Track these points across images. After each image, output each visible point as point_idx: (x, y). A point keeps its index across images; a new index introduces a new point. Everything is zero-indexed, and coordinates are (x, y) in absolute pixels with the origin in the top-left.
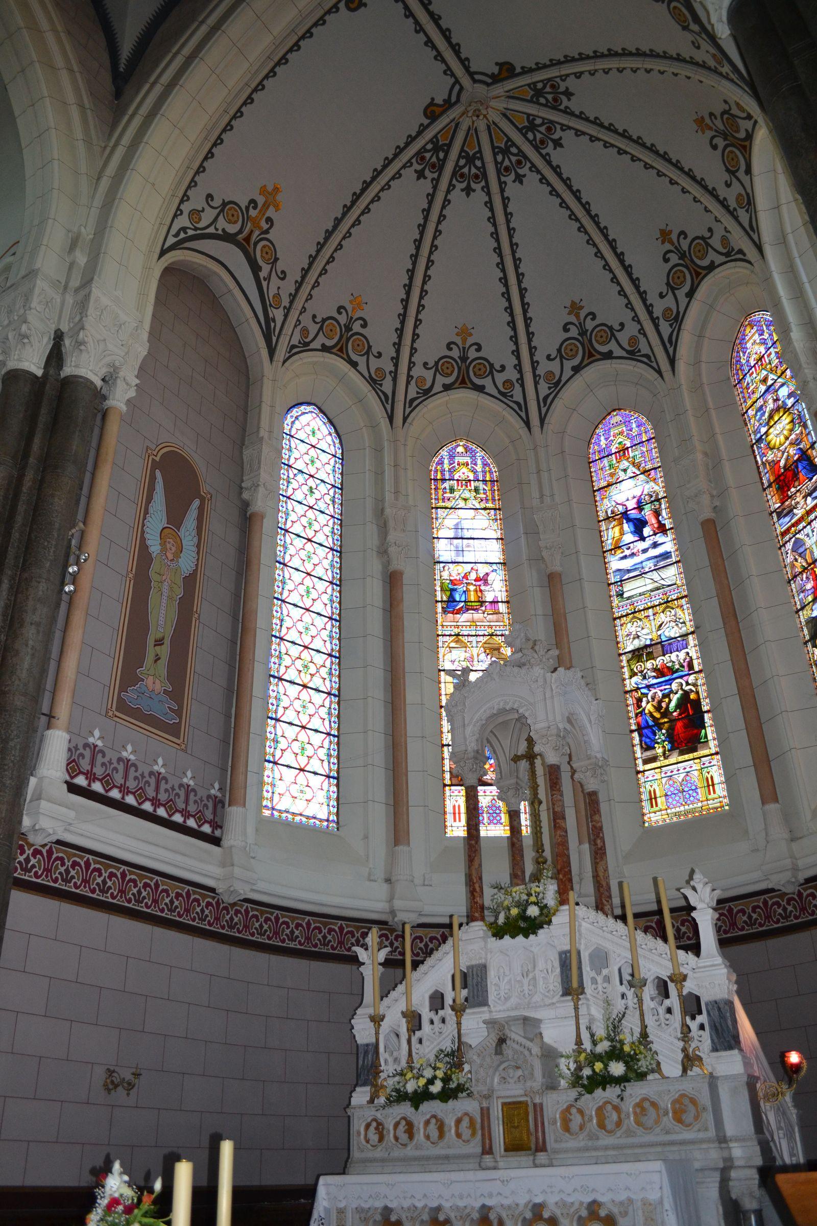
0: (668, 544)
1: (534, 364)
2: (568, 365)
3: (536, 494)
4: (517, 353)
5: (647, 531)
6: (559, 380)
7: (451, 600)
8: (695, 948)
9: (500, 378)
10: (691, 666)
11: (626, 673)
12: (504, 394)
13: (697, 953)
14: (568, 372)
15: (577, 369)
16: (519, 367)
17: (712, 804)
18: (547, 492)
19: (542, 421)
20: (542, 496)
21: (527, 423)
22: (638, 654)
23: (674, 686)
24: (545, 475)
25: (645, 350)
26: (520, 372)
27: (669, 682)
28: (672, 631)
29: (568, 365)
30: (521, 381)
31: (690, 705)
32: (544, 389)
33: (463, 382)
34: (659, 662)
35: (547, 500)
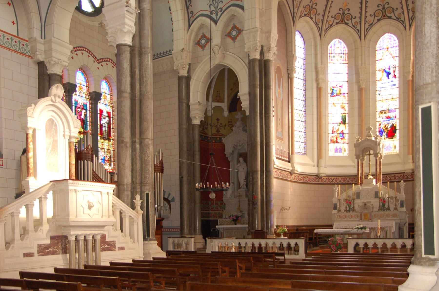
0: (396, 81)
1: (366, 17)
3: (360, 62)
4: (361, 13)
5: (390, 76)
6: (372, 23)
7: (332, 93)
8: (399, 192)
9: (354, 21)
10: (395, 117)
11: (377, 116)
12: (354, 26)
13: (400, 193)
14: (376, 21)
15: (379, 20)
16: (360, 18)
17: (394, 152)
18: (363, 62)
19: (365, 36)
20: (362, 64)
21: (360, 37)
22: (382, 112)
23: (390, 121)
24: (363, 56)
26: (361, 19)
27: (389, 120)
28: (392, 107)
30: (360, 22)
32: (367, 26)
33: (342, 21)
34: (388, 115)
35: (363, 65)
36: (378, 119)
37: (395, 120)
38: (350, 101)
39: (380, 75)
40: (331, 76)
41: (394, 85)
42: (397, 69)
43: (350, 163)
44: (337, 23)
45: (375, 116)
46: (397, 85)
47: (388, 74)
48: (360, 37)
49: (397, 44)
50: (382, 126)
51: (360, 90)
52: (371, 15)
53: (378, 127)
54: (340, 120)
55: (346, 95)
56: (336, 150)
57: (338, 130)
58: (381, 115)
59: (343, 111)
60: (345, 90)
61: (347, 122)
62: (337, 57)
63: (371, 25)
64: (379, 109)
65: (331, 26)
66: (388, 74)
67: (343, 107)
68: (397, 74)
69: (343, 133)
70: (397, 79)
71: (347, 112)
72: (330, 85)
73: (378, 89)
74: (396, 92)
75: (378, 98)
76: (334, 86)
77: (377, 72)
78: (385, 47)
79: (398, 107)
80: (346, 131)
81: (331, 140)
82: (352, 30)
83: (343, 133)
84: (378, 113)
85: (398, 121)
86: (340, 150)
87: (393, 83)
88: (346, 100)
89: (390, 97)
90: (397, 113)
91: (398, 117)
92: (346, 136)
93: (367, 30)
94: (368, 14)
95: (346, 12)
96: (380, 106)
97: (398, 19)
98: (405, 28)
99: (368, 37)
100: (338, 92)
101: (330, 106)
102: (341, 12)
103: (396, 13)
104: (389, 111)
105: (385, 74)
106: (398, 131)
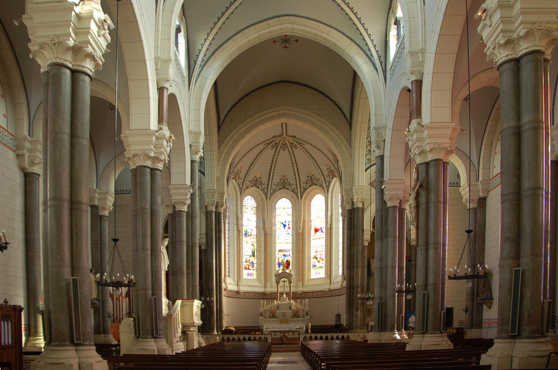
0: (290, 231)
1: (271, 185)
2: (278, 187)
4: (268, 182)
9: (263, 186)
11: (277, 253)
14: (278, 189)
15: (280, 189)
16: (268, 185)
21: (267, 198)
22: (280, 251)
25: (296, 192)
29: (278, 187)
30: (267, 188)
33: (255, 185)
34: (284, 253)
36: (277, 255)
38: (258, 241)
39: (279, 226)
40: (245, 222)
42: (291, 223)
44: (252, 186)
45: (275, 253)
46: (291, 234)
47: (285, 226)
48: (267, 198)
49: (291, 207)
50: (280, 261)
51: (266, 234)
55: (255, 237)
56: (248, 275)
58: (279, 253)
59: (253, 247)
60: (254, 232)
63: (275, 191)
65: (247, 187)
66: (285, 226)
67: (253, 245)
68: (291, 226)
70: (291, 230)
71: (255, 248)
72: (245, 228)
74: (290, 239)
75: (277, 241)
79: (291, 248)
80: (255, 262)
82: (261, 193)
84: (277, 251)
86: (251, 275)
88: (255, 240)
89: (286, 241)
90: (290, 253)
91: (291, 255)
92: (255, 265)
93: (271, 194)
96: (278, 247)
97: (293, 191)
99: (272, 198)
101: (244, 243)
102: (255, 179)
104: (285, 251)
105: (283, 226)
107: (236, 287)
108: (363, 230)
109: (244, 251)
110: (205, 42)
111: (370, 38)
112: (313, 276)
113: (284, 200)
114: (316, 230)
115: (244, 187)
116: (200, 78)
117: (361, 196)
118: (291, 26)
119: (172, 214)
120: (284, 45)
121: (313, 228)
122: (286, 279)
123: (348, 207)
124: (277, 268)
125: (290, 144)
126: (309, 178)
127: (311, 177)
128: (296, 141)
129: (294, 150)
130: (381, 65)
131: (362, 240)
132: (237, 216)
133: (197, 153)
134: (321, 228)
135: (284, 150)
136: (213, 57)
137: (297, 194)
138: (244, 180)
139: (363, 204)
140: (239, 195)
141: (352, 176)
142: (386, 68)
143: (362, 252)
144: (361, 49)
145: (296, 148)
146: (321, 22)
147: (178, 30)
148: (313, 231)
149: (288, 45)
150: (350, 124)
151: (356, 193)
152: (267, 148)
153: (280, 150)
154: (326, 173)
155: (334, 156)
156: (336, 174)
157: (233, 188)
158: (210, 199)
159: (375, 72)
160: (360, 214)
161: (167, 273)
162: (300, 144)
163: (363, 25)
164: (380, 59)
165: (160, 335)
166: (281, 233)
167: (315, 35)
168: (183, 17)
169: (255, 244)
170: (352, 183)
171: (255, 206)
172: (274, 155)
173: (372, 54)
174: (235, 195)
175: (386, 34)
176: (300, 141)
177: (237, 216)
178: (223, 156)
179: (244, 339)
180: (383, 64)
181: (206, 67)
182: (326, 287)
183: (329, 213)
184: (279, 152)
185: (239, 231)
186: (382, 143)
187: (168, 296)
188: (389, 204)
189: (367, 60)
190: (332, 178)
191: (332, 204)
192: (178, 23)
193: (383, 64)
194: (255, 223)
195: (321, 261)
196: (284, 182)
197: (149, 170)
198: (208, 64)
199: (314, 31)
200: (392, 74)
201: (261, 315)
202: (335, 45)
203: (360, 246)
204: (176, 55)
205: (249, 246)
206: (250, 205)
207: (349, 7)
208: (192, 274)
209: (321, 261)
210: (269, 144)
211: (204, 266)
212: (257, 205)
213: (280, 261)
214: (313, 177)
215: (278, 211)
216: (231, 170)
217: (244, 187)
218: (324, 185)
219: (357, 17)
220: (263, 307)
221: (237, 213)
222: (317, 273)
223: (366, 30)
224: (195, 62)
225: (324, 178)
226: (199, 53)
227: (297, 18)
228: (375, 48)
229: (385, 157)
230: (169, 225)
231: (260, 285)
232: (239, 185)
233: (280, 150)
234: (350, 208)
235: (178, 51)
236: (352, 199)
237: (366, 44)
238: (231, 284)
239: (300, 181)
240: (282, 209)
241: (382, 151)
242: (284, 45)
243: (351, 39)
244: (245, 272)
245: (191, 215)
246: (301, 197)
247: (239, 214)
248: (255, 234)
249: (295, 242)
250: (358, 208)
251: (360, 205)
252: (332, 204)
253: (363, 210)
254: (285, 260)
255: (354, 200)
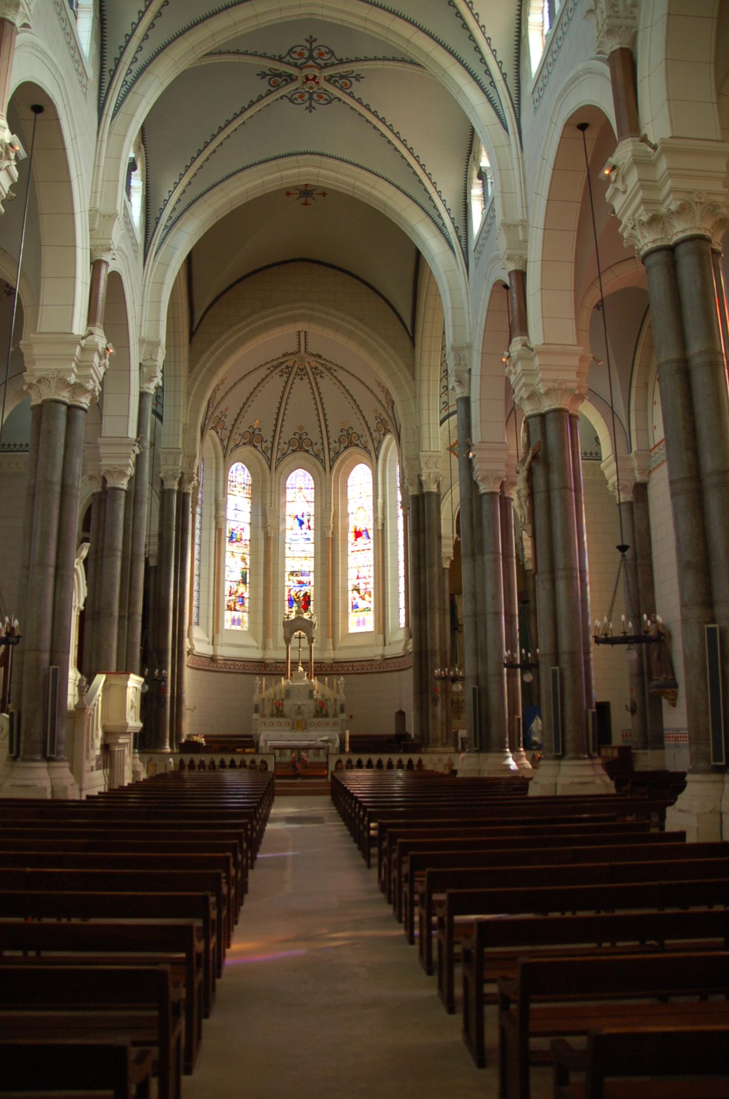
0: (311, 534)
1: (279, 443)
2: (291, 448)
4: (274, 437)
9: (264, 445)
11: (287, 578)
14: (290, 451)
15: (293, 451)
16: (273, 443)
22: (292, 573)
23: (303, 588)
29: (291, 448)
30: (272, 448)
31: (307, 597)
33: (250, 443)
36: (287, 583)
37: (309, 588)
38: (253, 553)
39: (291, 523)
40: (230, 514)
41: (309, 539)
42: (312, 518)
43: (251, 642)
44: (244, 444)
46: (312, 540)
49: (313, 486)
50: (293, 593)
51: (267, 539)
52: (285, 443)
53: (287, 593)
54: (239, 578)
55: (248, 543)
56: (234, 621)
57: (237, 592)
58: (291, 578)
59: (242, 565)
60: (247, 535)
61: (248, 581)
62: (239, 488)
64: (288, 569)
65: (237, 446)
66: (301, 523)
67: (244, 560)
69: (243, 597)
70: (312, 531)
71: (248, 567)
72: (230, 526)
73: (287, 540)
74: (310, 549)
75: (288, 553)
76: (234, 527)
77: (287, 518)
78: (297, 486)
79: (312, 569)
81: (228, 606)
82: (260, 456)
83: (242, 597)
84: (287, 574)
85: (313, 589)
87: (307, 536)
88: (247, 551)
90: (311, 578)
91: (312, 583)
92: (247, 602)
93: (279, 460)
94: (282, 441)
95: (257, 432)
96: (290, 565)
97: (316, 456)
98: (325, 469)
99: (279, 469)
100: (238, 537)
101: (228, 555)
102: (251, 431)
103: (316, 448)
106: (312, 603)
107: (211, 647)
108: (440, 537)
109: (227, 573)
110: (175, 188)
111: (440, 197)
112: (353, 628)
113: (300, 472)
114: (358, 534)
115: (232, 445)
116: (164, 247)
117: (437, 470)
118: (316, 170)
119: (100, 493)
120: (303, 200)
121: (351, 529)
122: (303, 633)
123: (413, 491)
124: (287, 610)
125: (311, 368)
126: (345, 433)
127: (347, 431)
128: (322, 365)
129: (319, 379)
130: (460, 241)
131: (440, 556)
132: (216, 501)
133: (151, 379)
134: (366, 530)
135: (302, 379)
136: (187, 214)
137: (322, 462)
138: (231, 431)
139: (438, 487)
140: (222, 459)
141: (417, 432)
142: (467, 248)
143: (439, 580)
144: (427, 213)
145: (322, 377)
146: (362, 167)
147: (132, 167)
148: (351, 536)
149: (309, 200)
150: (413, 339)
151: (426, 464)
152: (273, 374)
153: (294, 378)
154: (373, 425)
155: (387, 393)
156: (390, 427)
157: (211, 446)
158: (170, 467)
159: (450, 252)
160: (434, 504)
161: (82, 615)
162: (329, 369)
163: (429, 176)
164: (457, 232)
165: (59, 753)
166: (294, 537)
167: (354, 187)
168: (142, 146)
169: (248, 558)
170: (418, 445)
171: (249, 482)
172: (285, 388)
173: (444, 224)
174: (214, 460)
175: (466, 193)
176: (329, 365)
177: (216, 501)
178: (195, 388)
179: (223, 765)
180: (463, 240)
181: (175, 230)
182: (376, 652)
183: (380, 500)
184: (293, 383)
185: (219, 531)
186: (466, 375)
187: (80, 667)
188: (483, 489)
189: (437, 232)
190: (384, 435)
191: (384, 483)
192: (132, 155)
193: (463, 240)
194: (249, 516)
195: (367, 596)
196: (300, 438)
197: (63, 408)
198: (178, 225)
199: (352, 181)
200: (478, 259)
201: (256, 710)
202: (386, 205)
203: (436, 569)
204: (125, 208)
205: (236, 562)
206: (240, 479)
207: (406, 146)
208: (129, 618)
209: (367, 596)
210: (276, 367)
211: (151, 603)
212: (253, 481)
213: (293, 593)
214: (351, 432)
215: (290, 495)
216: (210, 413)
217: (232, 445)
218: (371, 447)
219: (418, 162)
220: (261, 692)
221: (217, 494)
222: (360, 621)
223: (434, 184)
224: (158, 220)
225: (371, 434)
226: (165, 205)
227: (324, 159)
228: (449, 214)
229: (472, 399)
230: (94, 516)
231: (256, 644)
232: (222, 440)
233: (294, 378)
234: (416, 493)
235: (129, 200)
236: (419, 476)
237: (435, 206)
238: (199, 640)
239: (328, 438)
240: (297, 490)
241: (467, 390)
242: (303, 200)
243: (411, 197)
244: (228, 615)
245: (133, 497)
246: (331, 468)
247: (221, 498)
248: (248, 537)
249: (319, 556)
250: (429, 494)
251: (434, 488)
252: (384, 483)
253: (438, 496)
254: (302, 594)
255: (423, 478)
